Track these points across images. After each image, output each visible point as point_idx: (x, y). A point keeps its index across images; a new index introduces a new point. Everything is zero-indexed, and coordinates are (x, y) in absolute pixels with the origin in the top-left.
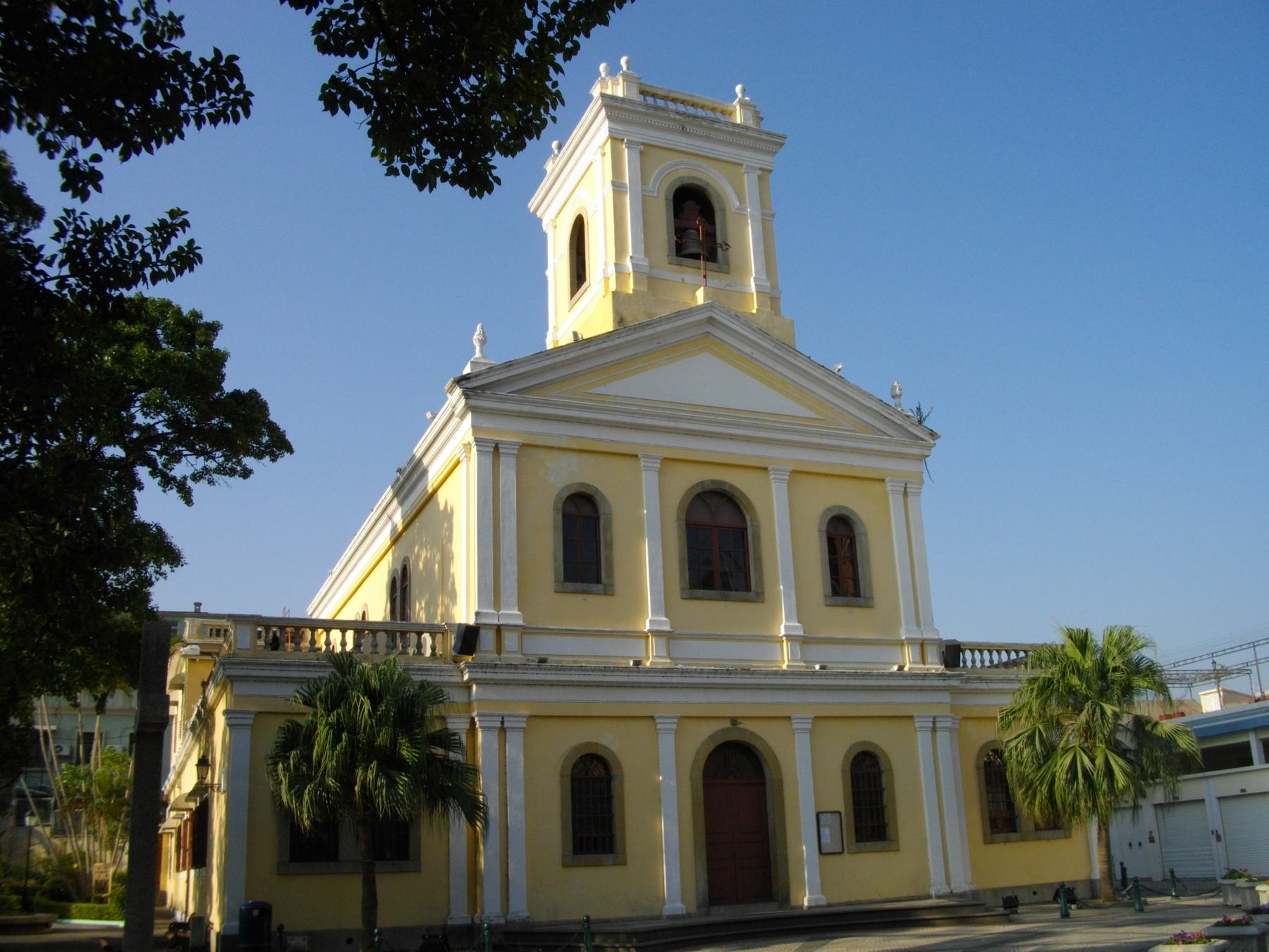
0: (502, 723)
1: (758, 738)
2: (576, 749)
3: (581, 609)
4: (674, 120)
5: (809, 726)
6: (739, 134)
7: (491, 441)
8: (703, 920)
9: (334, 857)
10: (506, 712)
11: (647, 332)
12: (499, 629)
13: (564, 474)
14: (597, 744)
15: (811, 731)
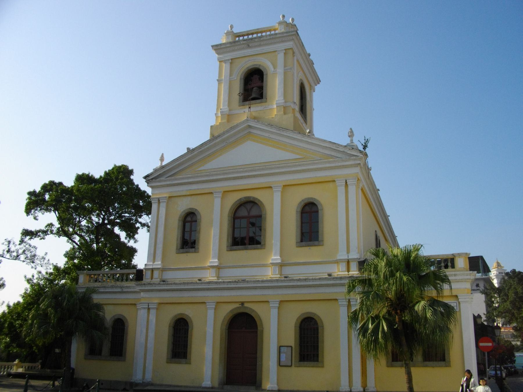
1: (253, 311)
3: (188, 259)
4: (243, 44)
5: (278, 305)
6: (273, 38)
7: (156, 198)
9: (100, 354)
12: (152, 270)
13: (183, 206)
14: (184, 314)
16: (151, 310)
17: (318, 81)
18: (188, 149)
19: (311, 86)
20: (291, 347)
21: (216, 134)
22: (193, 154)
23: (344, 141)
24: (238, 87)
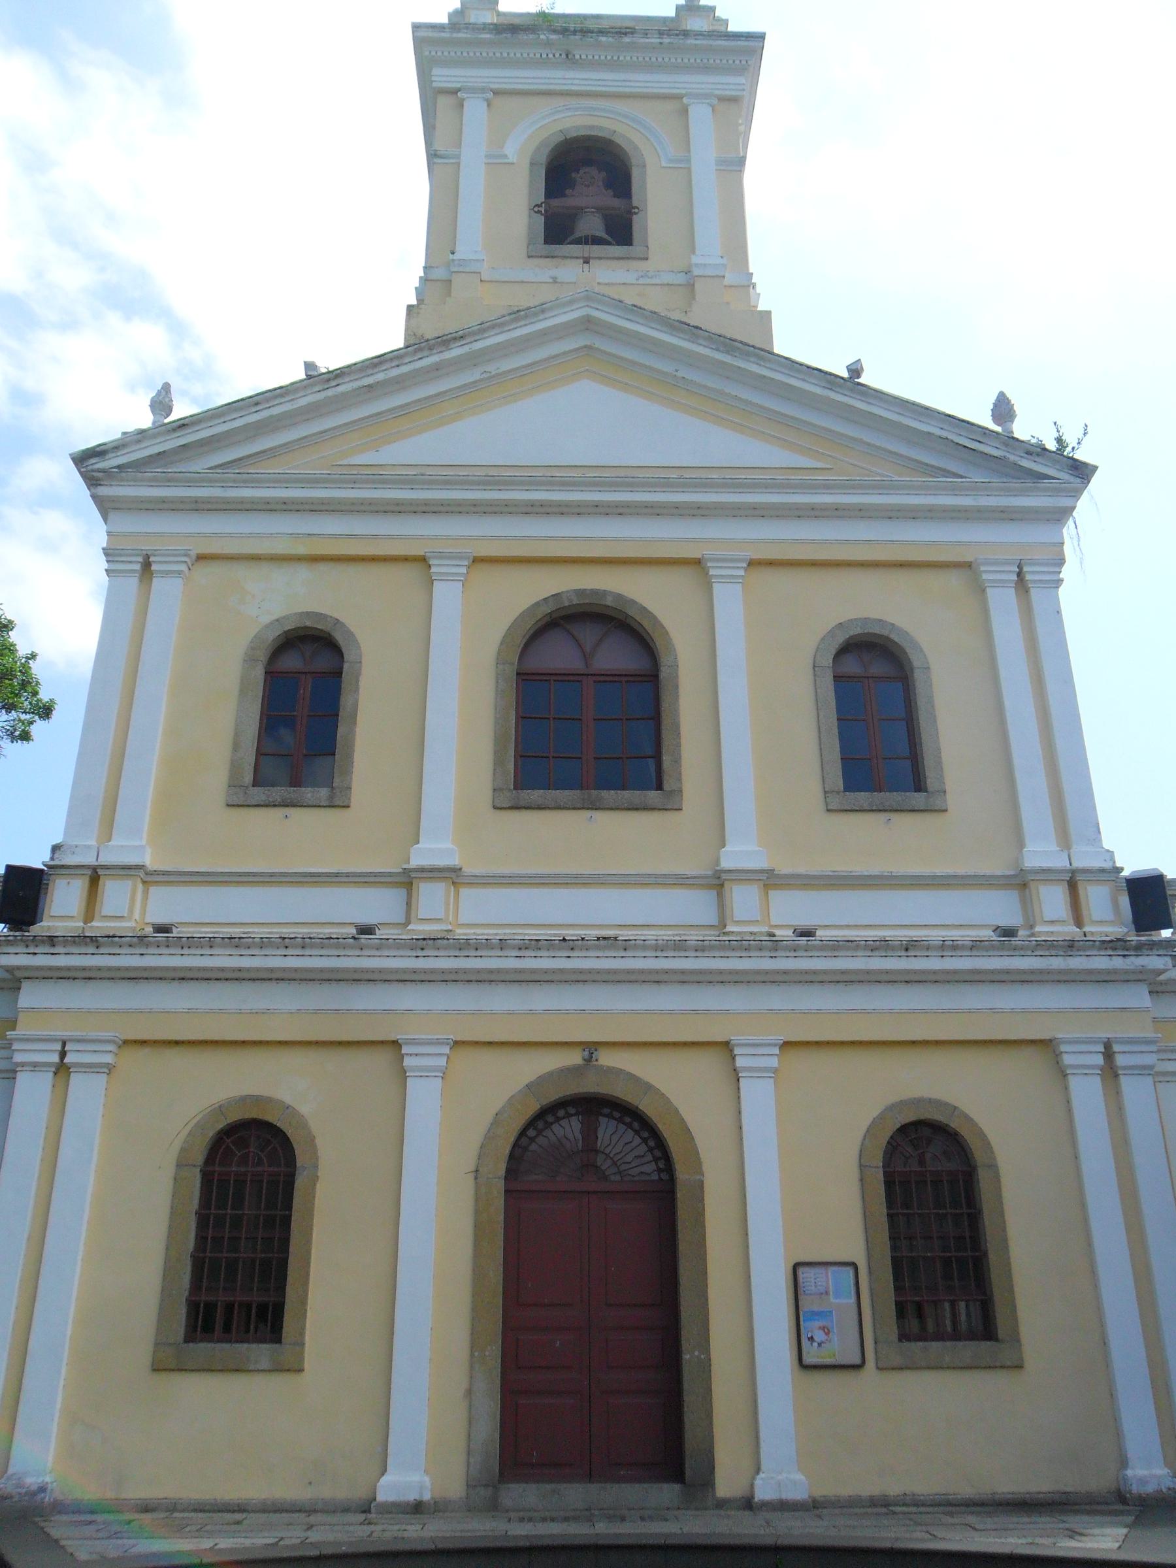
0: (63, 1054)
1: (649, 1088)
2: (221, 1109)
4: (548, 44)
10: (66, 1034)
11: (455, 352)
12: (95, 876)
13: (276, 599)
14: (269, 1100)
16: (75, 1079)
18: (309, 366)
20: (854, 1265)
22: (330, 393)
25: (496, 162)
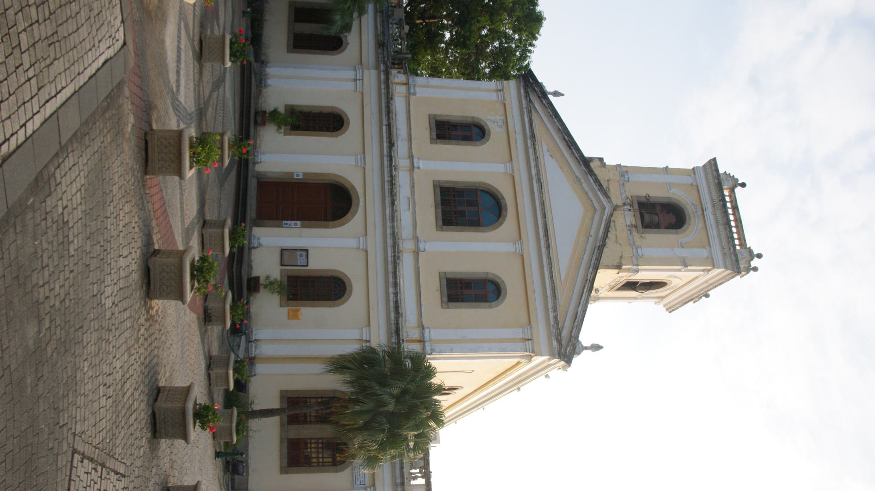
3: (422, 131)
8: (250, 173)
10: (365, 80)
15: (358, 248)
17: (671, 309)
19: (663, 297)
21: (592, 165)
23: (586, 337)
24: (657, 194)
25: (670, 185)
